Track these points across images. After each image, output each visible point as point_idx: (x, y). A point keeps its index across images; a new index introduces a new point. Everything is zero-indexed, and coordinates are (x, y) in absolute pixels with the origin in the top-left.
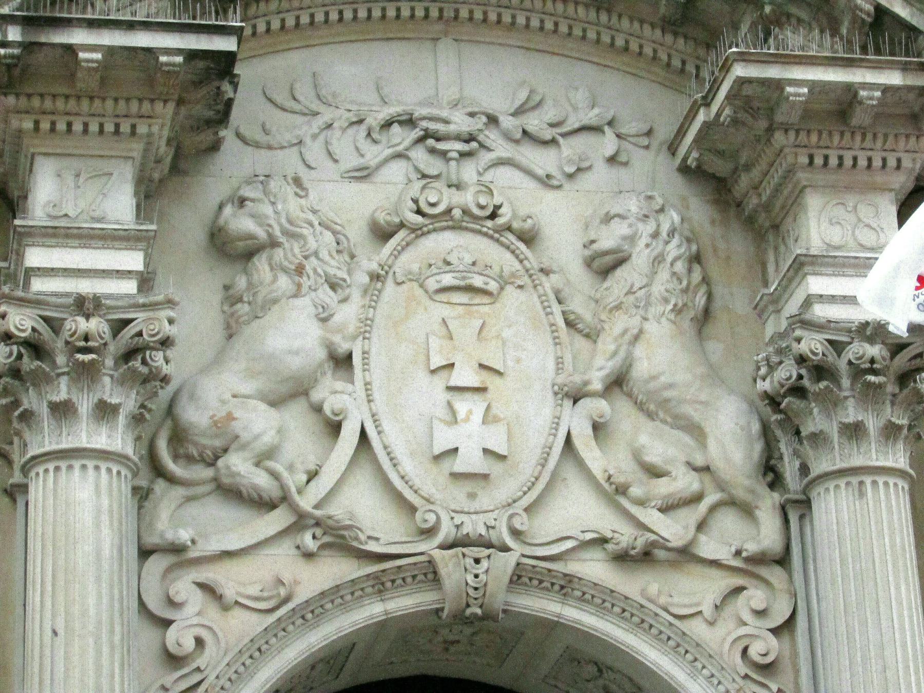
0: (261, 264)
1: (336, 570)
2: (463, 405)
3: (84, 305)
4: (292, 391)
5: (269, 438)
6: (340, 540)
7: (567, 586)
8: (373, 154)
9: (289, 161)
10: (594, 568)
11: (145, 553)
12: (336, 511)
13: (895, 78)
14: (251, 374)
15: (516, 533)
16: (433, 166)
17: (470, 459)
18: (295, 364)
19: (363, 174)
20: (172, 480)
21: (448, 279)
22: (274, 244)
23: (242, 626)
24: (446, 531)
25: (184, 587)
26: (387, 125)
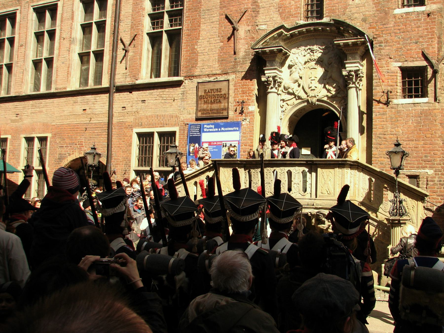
0: (293, 67)
1: (300, 101)
2: (312, 81)
3: (269, 77)
4: (296, 81)
5: (292, 88)
6: (299, 98)
7: (323, 101)
8: (306, 53)
9: (297, 56)
10: (325, 99)
11: (281, 100)
12: (299, 95)
13: (353, 41)
14: (291, 80)
15: (318, 96)
16: (312, 54)
17: (313, 88)
18: (296, 79)
19: (305, 56)
20: (284, 92)
21: (312, 67)
22: (294, 65)
23: (290, 107)
24: (310, 96)
25: (284, 104)
26: (307, 50)
